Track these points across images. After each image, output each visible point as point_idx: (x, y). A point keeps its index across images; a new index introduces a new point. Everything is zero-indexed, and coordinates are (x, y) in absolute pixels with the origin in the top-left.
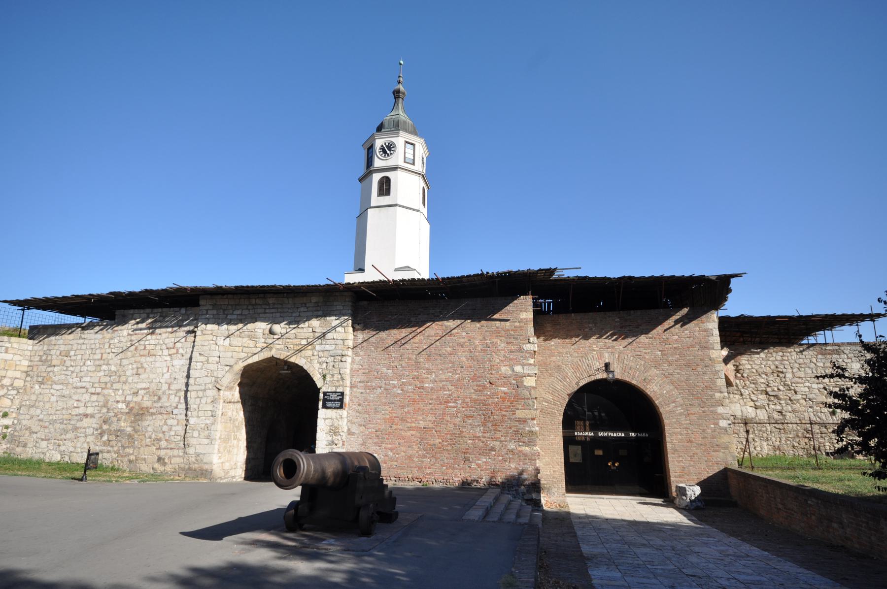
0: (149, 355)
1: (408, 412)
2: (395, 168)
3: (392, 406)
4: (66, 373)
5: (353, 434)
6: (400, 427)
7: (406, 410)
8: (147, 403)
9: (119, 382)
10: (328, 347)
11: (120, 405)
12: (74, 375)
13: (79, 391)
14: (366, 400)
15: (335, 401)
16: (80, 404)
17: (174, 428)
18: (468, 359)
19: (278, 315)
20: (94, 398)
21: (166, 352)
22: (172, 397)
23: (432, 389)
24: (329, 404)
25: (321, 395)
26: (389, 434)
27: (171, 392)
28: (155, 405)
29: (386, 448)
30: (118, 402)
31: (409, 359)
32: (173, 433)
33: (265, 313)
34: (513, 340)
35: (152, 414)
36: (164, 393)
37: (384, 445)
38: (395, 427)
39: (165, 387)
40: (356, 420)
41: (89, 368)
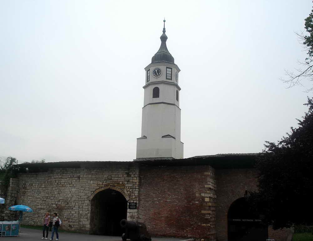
0: (63, 186)
3: (155, 208)
4: (33, 192)
8: (63, 205)
9: (52, 196)
12: (35, 193)
13: (38, 199)
15: (133, 206)
16: (38, 204)
17: (74, 215)
20: (44, 202)
21: (69, 186)
23: (170, 202)
24: (131, 207)
25: (128, 204)
26: (154, 219)
27: (72, 201)
28: (66, 206)
30: (53, 204)
32: (74, 216)
34: (201, 183)
35: (66, 209)
39: (69, 199)
41: (41, 191)
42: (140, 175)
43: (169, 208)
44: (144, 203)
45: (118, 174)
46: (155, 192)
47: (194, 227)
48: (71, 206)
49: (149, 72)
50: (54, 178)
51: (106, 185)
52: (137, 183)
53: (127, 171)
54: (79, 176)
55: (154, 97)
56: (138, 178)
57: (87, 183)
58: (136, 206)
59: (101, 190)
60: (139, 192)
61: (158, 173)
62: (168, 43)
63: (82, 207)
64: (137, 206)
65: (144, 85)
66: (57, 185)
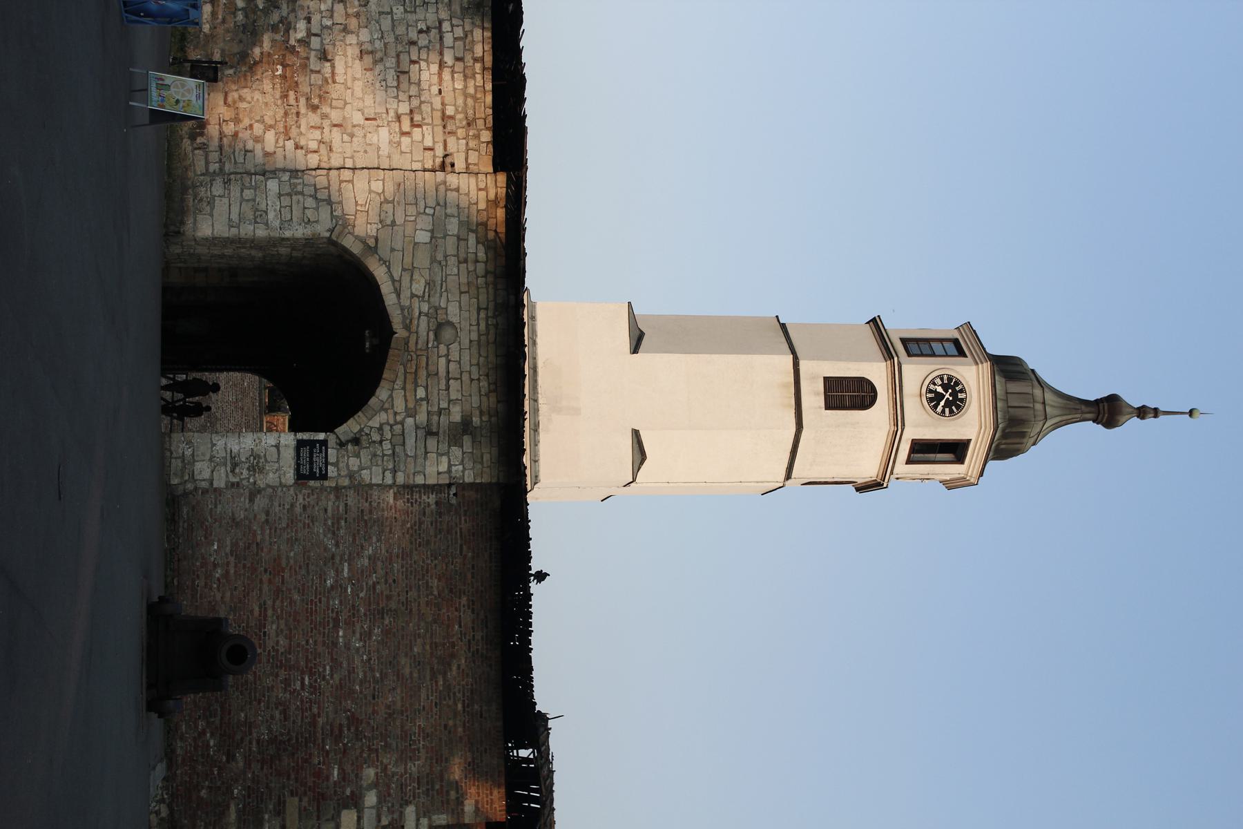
1: (292, 602)
2: (898, 420)
3: (303, 572)
5: (251, 500)
6: (265, 587)
7: (296, 597)
9: (347, 15)
10: (410, 442)
11: (302, 25)
14: (313, 519)
15: (311, 463)
18: (388, 707)
19: (474, 336)
21: (404, 108)
22: (317, 134)
23: (335, 644)
24: (305, 452)
25: (321, 436)
27: (326, 130)
28: (303, 101)
29: (228, 564)
30: (309, 20)
31: (389, 598)
33: (479, 309)
35: (285, 96)
36: (325, 116)
37: (232, 559)
38: (266, 577)
39: (335, 116)
40: (276, 504)
42: (463, 487)
43: (307, 642)
44: (326, 510)
45: (465, 377)
46: (379, 564)
47: (220, 769)
48: (303, 129)
49: (951, 348)
50: (440, 23)
51: (406, 311)
52: (419, 480)
53: (476, 420)
54: (453, 165)
55: (825, 378)
56: (445, 480)
57: (419, 213)
58: (312, 476)
59: (386, 289)
60: (378, 485)
61: (469, 575)
62: (1089, 429)
63: (297, 193)
64: (312, 483)
65: (889, 324)
66: (406, 39)
